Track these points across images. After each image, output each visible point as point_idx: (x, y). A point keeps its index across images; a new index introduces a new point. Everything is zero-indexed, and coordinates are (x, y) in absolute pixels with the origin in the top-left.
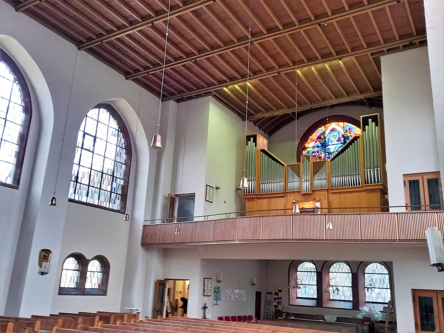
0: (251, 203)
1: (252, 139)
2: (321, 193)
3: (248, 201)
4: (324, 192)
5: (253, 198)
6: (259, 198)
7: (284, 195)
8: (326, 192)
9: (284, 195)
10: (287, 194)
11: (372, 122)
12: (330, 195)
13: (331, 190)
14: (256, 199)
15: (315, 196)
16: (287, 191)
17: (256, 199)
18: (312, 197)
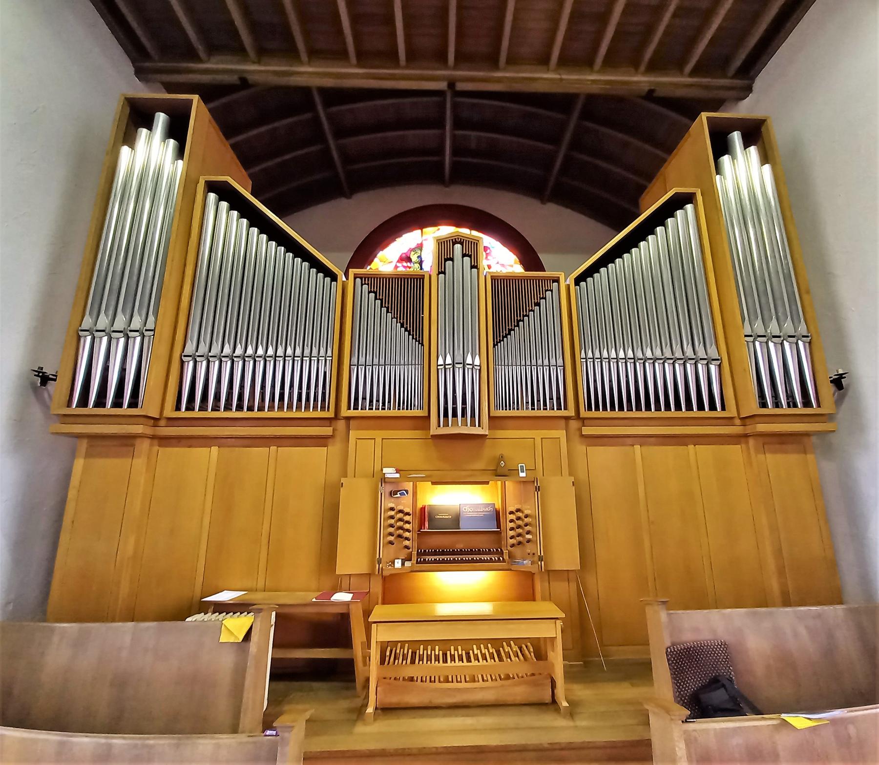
0: (110, 466)
1: (161, 118)
2: (538, 434)
3: (88, 455)
4: (554, 433)
5: (128, 440)
6: (165, 441)
7: (327, 431)
8: (561, 434)
9: (327, 431)
10: (341, 424)
11: (746, 145)
12: (580, 448)
13: (584, 421)
14: (144, 446)
15: (504, 449)
16: (345, 412)
17: (144, 446)
18: (489, 451)
